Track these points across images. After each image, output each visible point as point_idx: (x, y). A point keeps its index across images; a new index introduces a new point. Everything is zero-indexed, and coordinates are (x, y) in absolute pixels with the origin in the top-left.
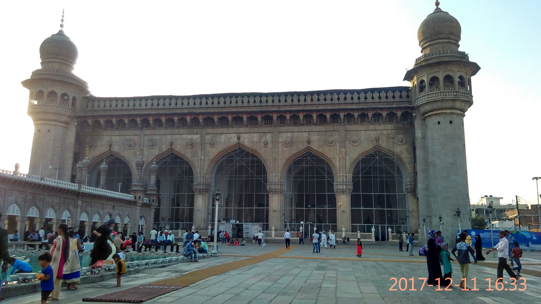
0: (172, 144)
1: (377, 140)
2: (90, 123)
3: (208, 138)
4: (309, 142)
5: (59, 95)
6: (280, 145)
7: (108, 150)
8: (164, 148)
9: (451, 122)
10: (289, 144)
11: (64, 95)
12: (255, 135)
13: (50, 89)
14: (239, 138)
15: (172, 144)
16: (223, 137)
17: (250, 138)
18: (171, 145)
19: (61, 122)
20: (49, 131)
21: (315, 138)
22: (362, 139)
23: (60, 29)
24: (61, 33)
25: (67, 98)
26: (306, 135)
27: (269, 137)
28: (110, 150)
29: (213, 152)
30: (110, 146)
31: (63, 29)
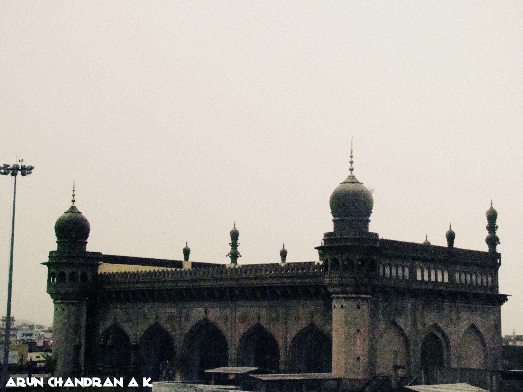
0: (157, 317)
1: (312, 316)
3: (183, 310)
4: (259, 319)
6: (237, 321)
8: (153, 322)
9: (342, 307)
10: (244, 318)
11: (72, 274)
14: (206, 313)
17: (215, 313)
19: (72, 300)
20: (63, 310)
21: (263, 314)
22: (300, 316)
23: (71, 204)
24: (73, 209)
26: (256, 310)
27: (228, 311)
29: (188, 326)
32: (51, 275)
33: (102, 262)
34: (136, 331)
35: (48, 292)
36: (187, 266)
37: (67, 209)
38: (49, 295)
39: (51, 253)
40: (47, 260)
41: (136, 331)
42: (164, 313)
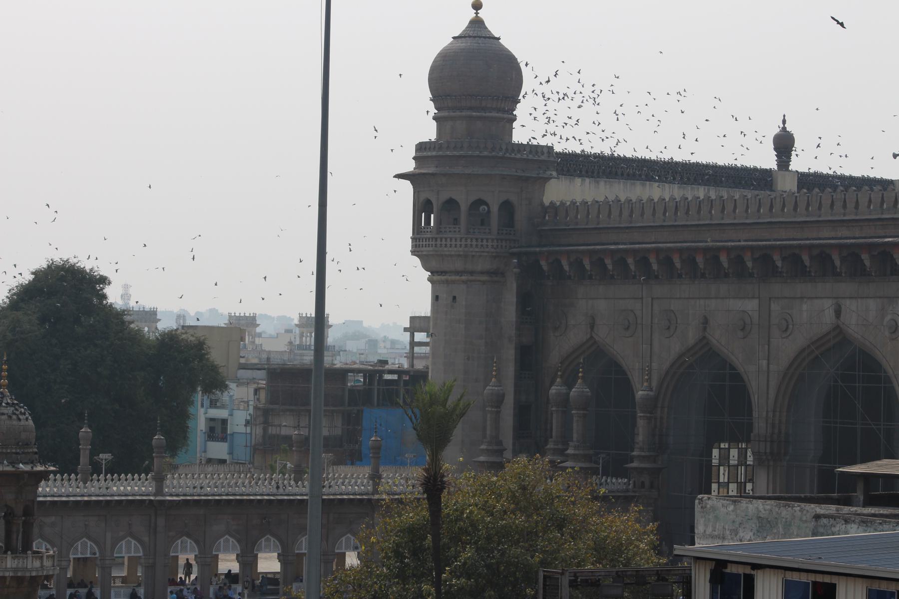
0: (706, 322)
2: (545, 268)
3: (775, 307)
5: (464, 207)
7: (589, 336)
11: (480, 202)
12: (872, 304)
13: (445, 196)
14: (838, 313)
15: (706, 322)
16: (805, 307)
18: (705, 329)
20: (454, 298)
23: (472, 14)
25: (483, 208)
28: (592, 337)
29: (788, 348)
30: (592, 327)
31: (482, 14)
32: (422, 207)
33: (554, 174)
34: (648, 360)
35: (414, 253)
36: (788, 185)
37: (460, 26)
38: (417, 261)
39: (421, 147)
40: (410, 166)
41: (648, 360)
42: (723, 312)
